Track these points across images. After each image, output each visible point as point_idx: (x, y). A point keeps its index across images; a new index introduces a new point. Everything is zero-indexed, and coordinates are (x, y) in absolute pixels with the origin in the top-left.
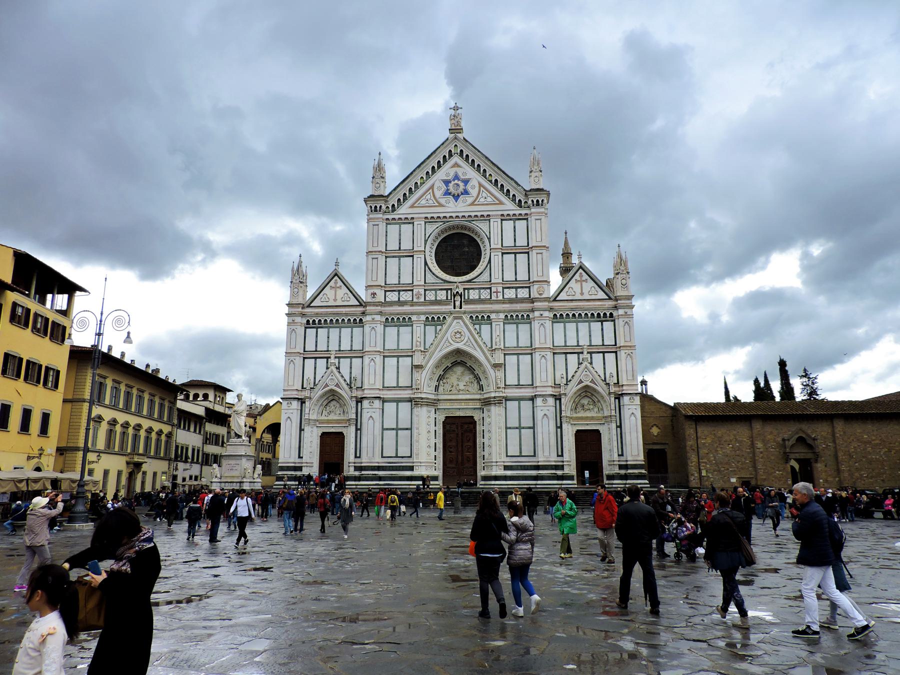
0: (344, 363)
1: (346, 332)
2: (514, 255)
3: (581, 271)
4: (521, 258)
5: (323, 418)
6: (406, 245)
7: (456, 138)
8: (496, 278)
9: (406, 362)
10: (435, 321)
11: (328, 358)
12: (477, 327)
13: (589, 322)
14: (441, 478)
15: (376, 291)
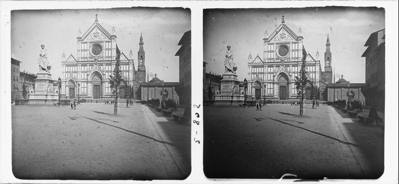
0: (260, 75)
1: (260, 68)
2: (294, 52)
3: (309, 55)
4: (296, 52)
5: (256, 86)
6: (272, 50)
7: (283, 24)
8: (291, 57)
9: (272, 75)
10: (278, 66)
11: (257, 74)
12: (287, 67)
13: (310, 66)
14: (279, 98)
15: (266, 60)
